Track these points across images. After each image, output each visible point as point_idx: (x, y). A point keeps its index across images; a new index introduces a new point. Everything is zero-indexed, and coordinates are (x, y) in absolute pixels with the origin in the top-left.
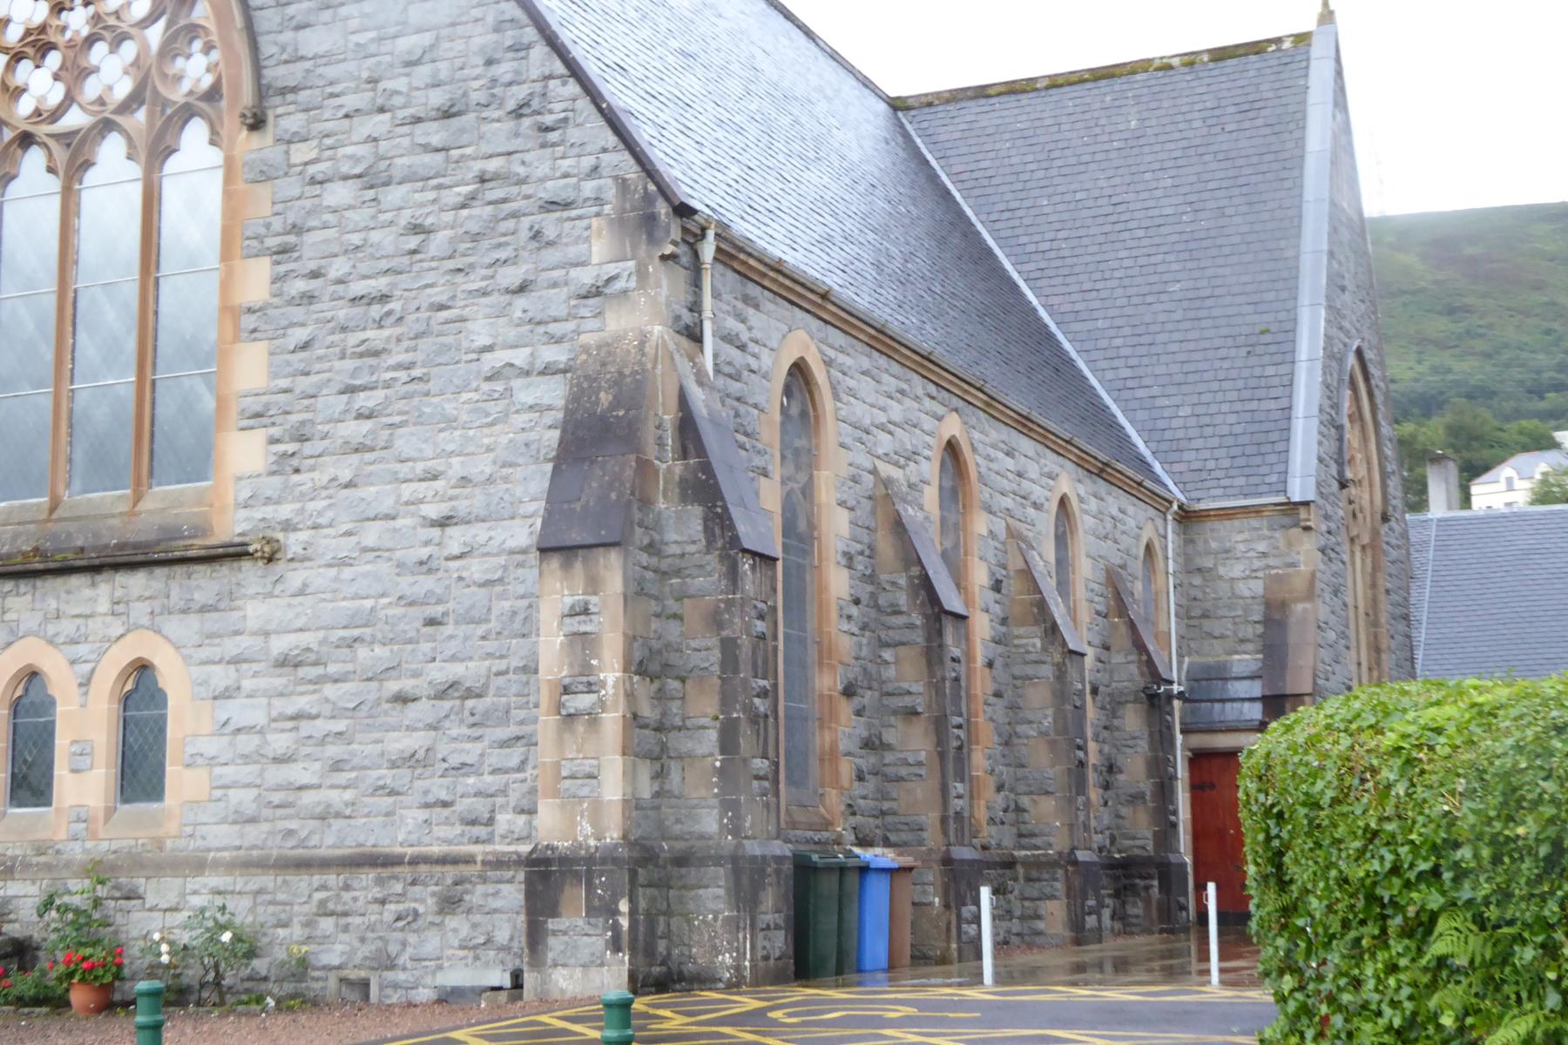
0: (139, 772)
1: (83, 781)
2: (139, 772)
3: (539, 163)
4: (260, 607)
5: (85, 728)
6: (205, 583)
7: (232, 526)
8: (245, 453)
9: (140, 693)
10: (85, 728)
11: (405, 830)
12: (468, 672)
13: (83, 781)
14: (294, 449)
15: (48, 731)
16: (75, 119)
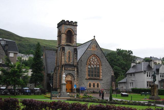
0: (98, 86)
1: (96, 87)
2: (98, 86)
3: (110, 69)
4: (102, 82)
5: (96, 85)
6: (100, 81)
7: (101, 79)
8: (101, 77)
9: (98, 84)
10: (96, 85)
11: (107, 89)
12: (109, 84)
13: (96, 87)
14: (103, 77)
15: (94, 85)
16: (94, 64)
